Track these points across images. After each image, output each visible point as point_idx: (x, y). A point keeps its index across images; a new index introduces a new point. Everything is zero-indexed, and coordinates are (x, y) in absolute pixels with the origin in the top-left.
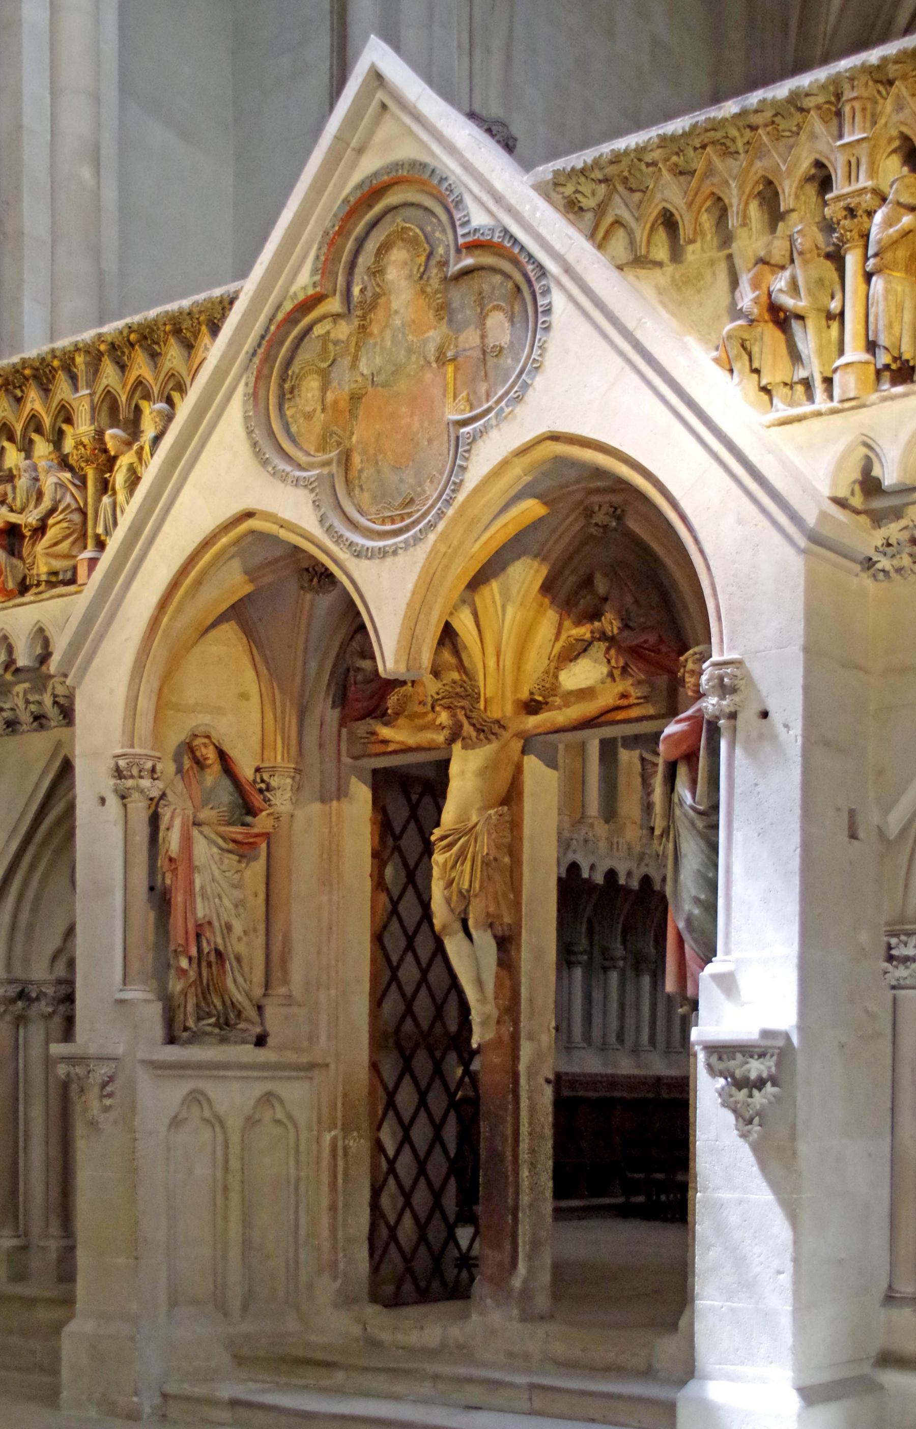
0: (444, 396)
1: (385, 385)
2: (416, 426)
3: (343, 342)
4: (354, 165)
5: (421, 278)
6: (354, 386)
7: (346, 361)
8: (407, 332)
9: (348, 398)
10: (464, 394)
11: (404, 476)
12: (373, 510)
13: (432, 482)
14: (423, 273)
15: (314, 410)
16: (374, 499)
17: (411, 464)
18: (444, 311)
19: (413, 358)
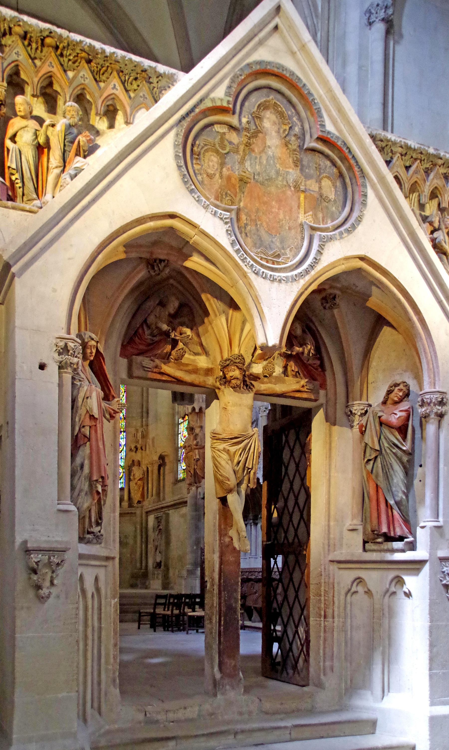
0: (299, 207)
1: (262, 184)
2: (281, 216)
3: (234, 144)
4: (255, 49)
5: (285, 137)
6: (244, 174)
7: (237, 157)
8: (276, 162)
9: (238, 180)
10: (311, 213)
11: (274, 240)
12: (253, 249)
13: (291, 250)
14: (287, 135)
15: (215, 175)
16: (255, 245)
17: (278, 235)
18: (297, 163)
19: (280, 178)
